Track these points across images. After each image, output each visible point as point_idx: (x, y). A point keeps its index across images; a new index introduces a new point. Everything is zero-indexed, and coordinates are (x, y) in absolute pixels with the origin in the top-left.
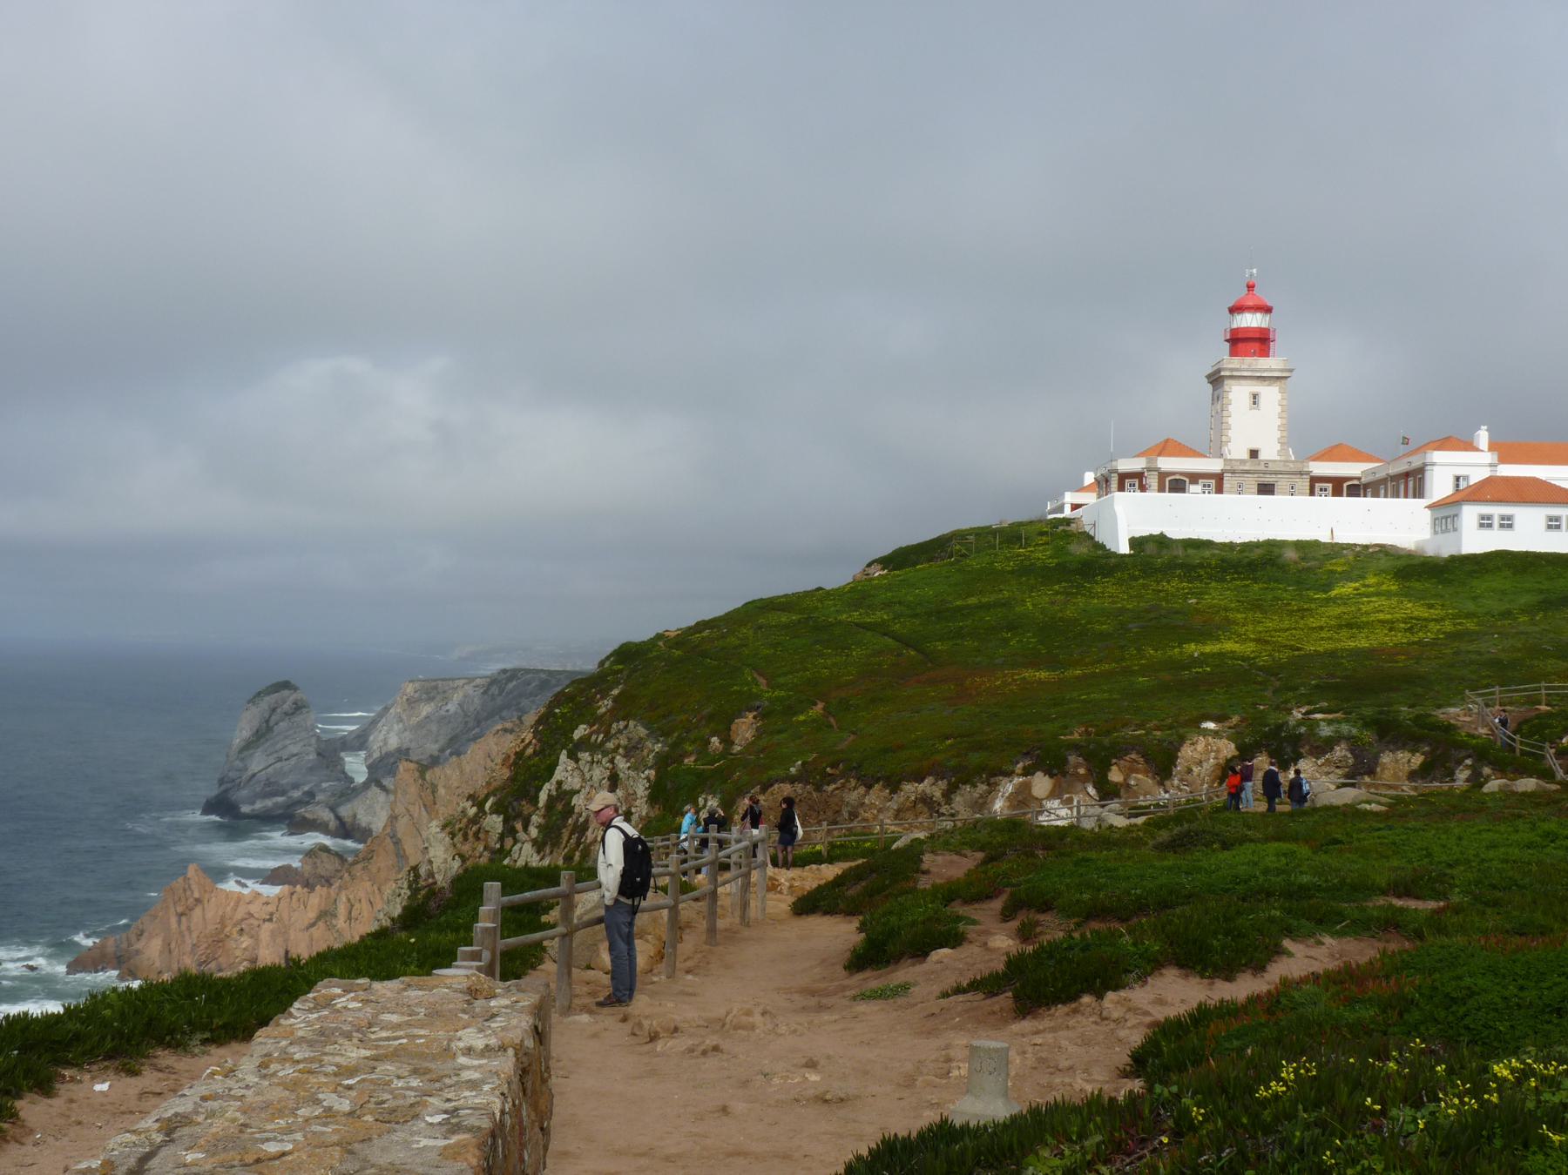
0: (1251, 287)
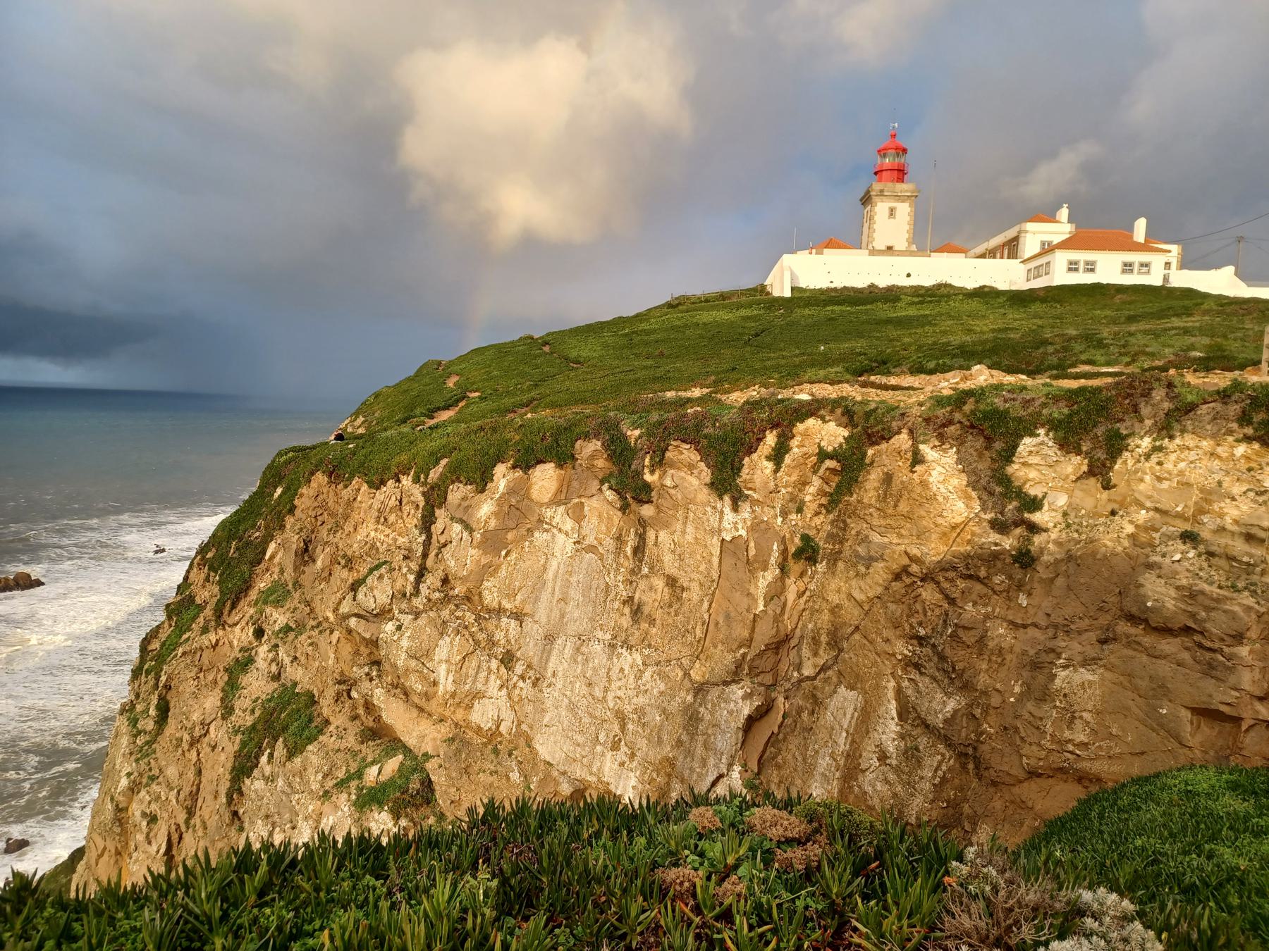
0: (894, 136)
